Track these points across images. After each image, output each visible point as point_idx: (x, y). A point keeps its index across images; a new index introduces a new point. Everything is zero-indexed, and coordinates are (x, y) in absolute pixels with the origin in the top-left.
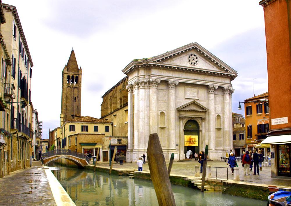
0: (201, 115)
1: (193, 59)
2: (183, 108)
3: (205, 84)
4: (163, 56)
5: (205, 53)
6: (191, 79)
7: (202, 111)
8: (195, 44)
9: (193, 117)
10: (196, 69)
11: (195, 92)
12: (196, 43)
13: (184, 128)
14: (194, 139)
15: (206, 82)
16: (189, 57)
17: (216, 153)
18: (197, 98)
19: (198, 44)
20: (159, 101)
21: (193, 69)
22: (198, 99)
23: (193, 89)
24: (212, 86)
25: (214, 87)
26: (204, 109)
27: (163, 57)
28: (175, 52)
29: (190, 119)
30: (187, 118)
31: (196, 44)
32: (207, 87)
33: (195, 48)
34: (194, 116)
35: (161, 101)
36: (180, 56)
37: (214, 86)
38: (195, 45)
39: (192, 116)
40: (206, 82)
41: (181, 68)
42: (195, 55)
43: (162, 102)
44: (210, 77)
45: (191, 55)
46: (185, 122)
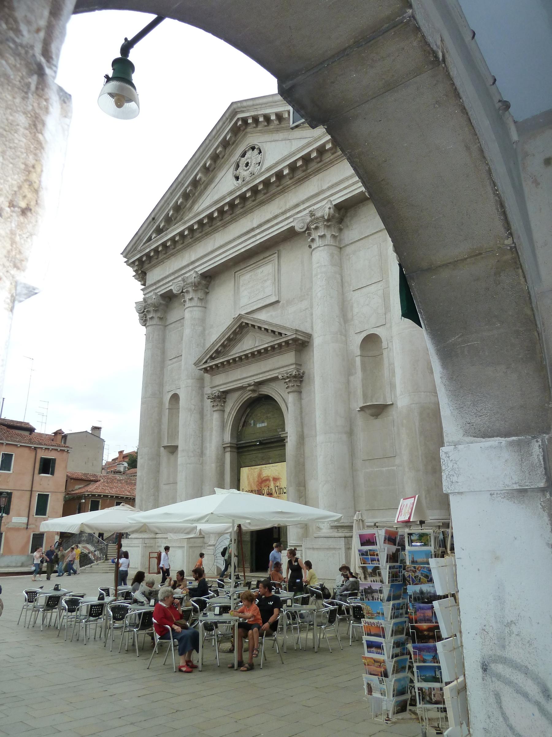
0: (284, 363)
1: (247, 165)
2: (212, 358)
3: (284, 226)
4: (153, 219)
5: (267, 111)
6: (234, 240)
7: (273, 347)
8: (233, 110)
9: (250, 385)
10: (238, 194)
11: (265, 281)
12: (232, 103)
13: (228, 438)
14: (275, 479)
15: (288, 215)
16: (238, 166)
17: (329, 549)
18: (273, 299)
19: (239, 105)
20: (170, 362)
21: (228, 200)
22: (277, 302)
23: (260, 270)
24: (309, 219)
25: (319, 214)
26: (280, 334)
27: (157, 224)
28: (183, 184)
29: (248, 395)
30: (237, 395)
31: (235, 106)
32: (290, 236)
33: (240, 123)
34: (251, 380)
35: (174, 360)
36: (213, 186)
37: (312, 214)
38: (235, 113)
39: (244, 383)
40: (288, 215)
41: (195, 223)
42: (253, 148)
43: (176, 362)
44: (307, 182)
45: (243, 155)
46: (234, 413)
